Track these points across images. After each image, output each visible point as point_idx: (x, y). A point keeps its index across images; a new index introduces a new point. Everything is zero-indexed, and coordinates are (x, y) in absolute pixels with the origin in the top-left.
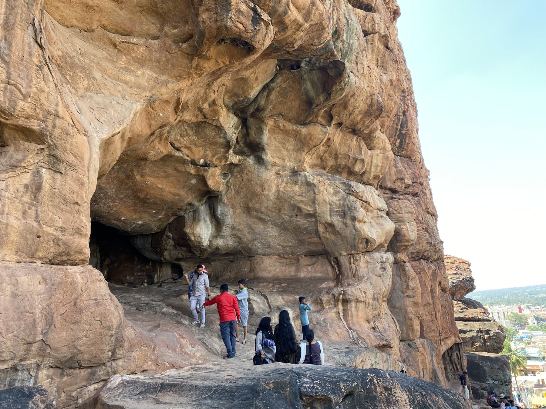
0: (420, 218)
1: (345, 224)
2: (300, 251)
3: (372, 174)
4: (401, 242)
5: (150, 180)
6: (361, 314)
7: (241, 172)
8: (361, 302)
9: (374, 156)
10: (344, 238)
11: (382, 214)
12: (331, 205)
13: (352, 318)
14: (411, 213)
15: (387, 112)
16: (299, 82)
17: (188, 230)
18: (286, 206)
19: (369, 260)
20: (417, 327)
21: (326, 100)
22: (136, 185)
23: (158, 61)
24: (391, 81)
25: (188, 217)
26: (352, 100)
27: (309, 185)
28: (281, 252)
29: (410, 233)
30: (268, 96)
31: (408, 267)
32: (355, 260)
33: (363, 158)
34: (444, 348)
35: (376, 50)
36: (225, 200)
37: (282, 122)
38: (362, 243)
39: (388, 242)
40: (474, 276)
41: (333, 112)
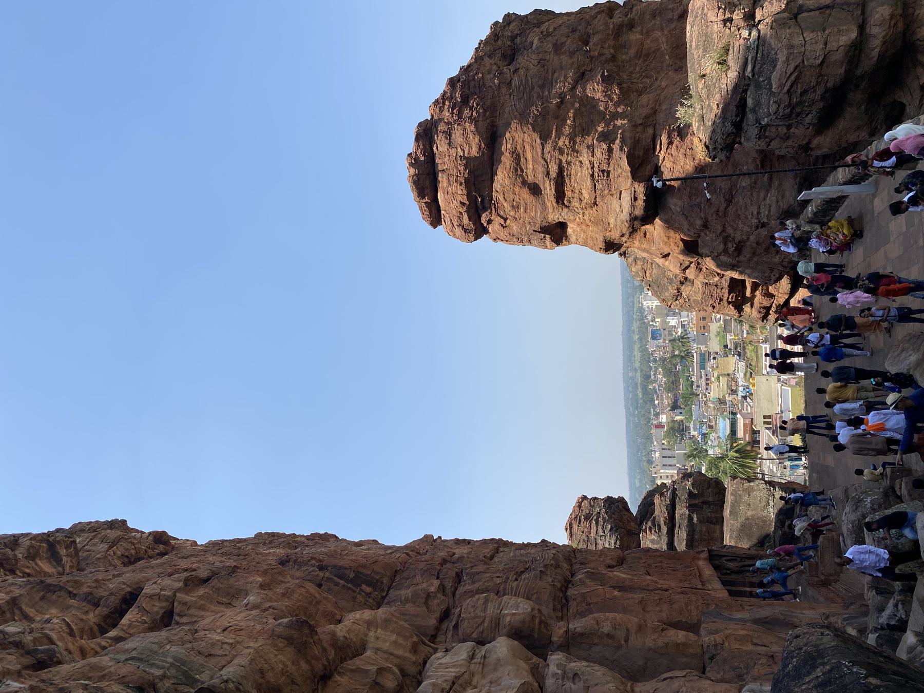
0: (498, 581)
3: (408, 655)
9: (377, 646)
14: (487, 600)
15: (311, 603)
20: (680, 636)
24: (262, 586)
29: (520, 611)
31: (577, 625)
33: (374, 668)
34: (718, 590)
39: (530, 654)
40: (602, 496)
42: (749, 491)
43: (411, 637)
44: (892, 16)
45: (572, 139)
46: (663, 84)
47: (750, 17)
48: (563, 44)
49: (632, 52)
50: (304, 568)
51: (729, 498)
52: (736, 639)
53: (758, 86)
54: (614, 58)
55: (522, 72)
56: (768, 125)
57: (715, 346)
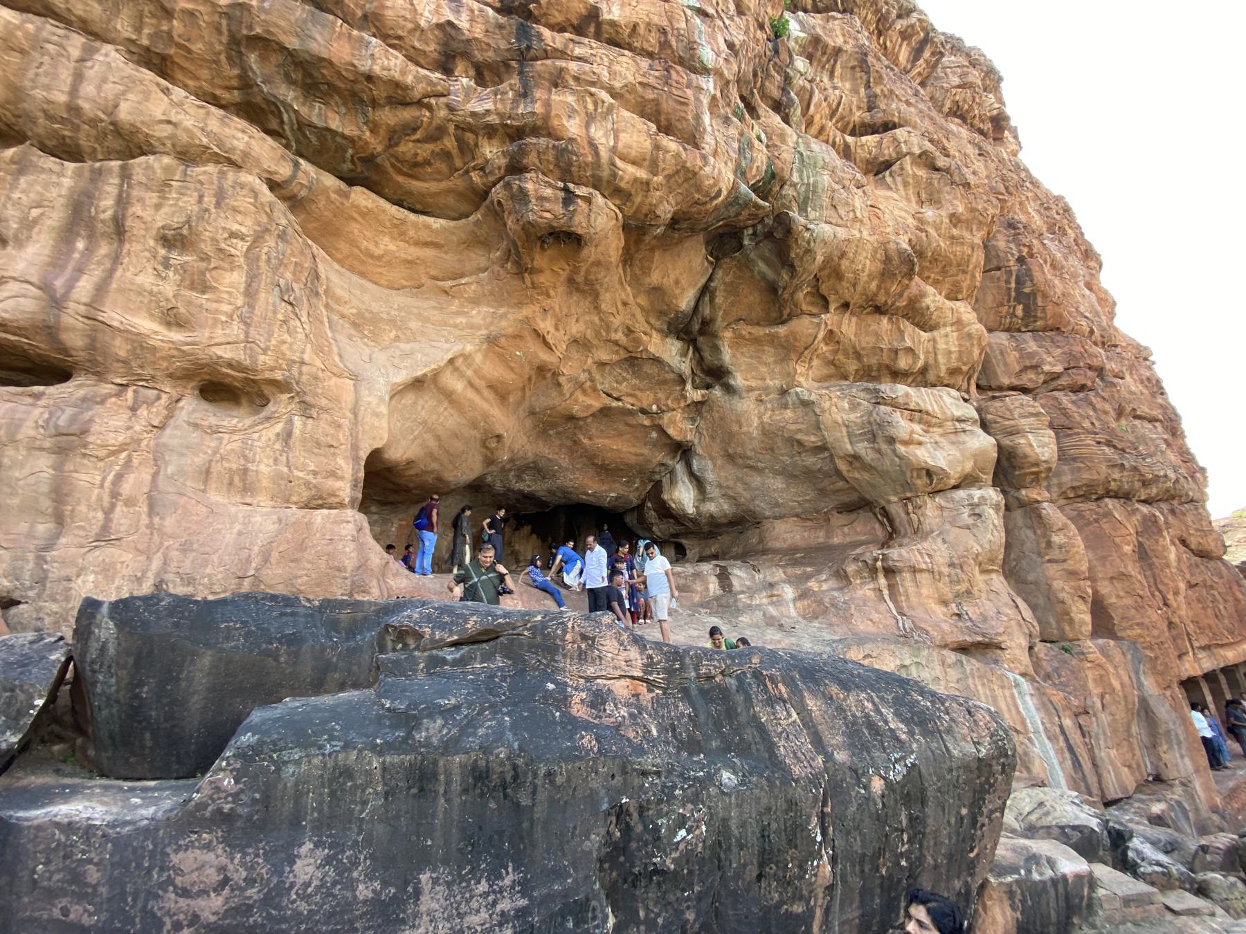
1: (879, 451)
2: (827, 505)
4: (1021, 468)
5: (601, 442)
6: (925, 591)
7: (711, 409)
8: (921, 571)
10: (883, 474)
11: (963, 425)
12: (847, 427)
13: (908, 597)
14: (1036, 415)
16: (747, 267)
17: (665, 497)
18: (779, 442)
19: (943, 504)
20: (1082, 615)
21: (792, 277)
22: (586, 451)
23: (491, 294)
25: (666, 481)
26: (845, 264)
27: (806, 404)
28: (799, 510)
29: (1038, 450)
30: (712, 300)
32: (915, 508)
33: (909, 343)
35: (911, 181)
36: (699, 450)
37: (745, 330)
38: (919, 477)
41: (824, 289)
43: (965, 364)
50: (1012, 245)
52: (1101, 676)
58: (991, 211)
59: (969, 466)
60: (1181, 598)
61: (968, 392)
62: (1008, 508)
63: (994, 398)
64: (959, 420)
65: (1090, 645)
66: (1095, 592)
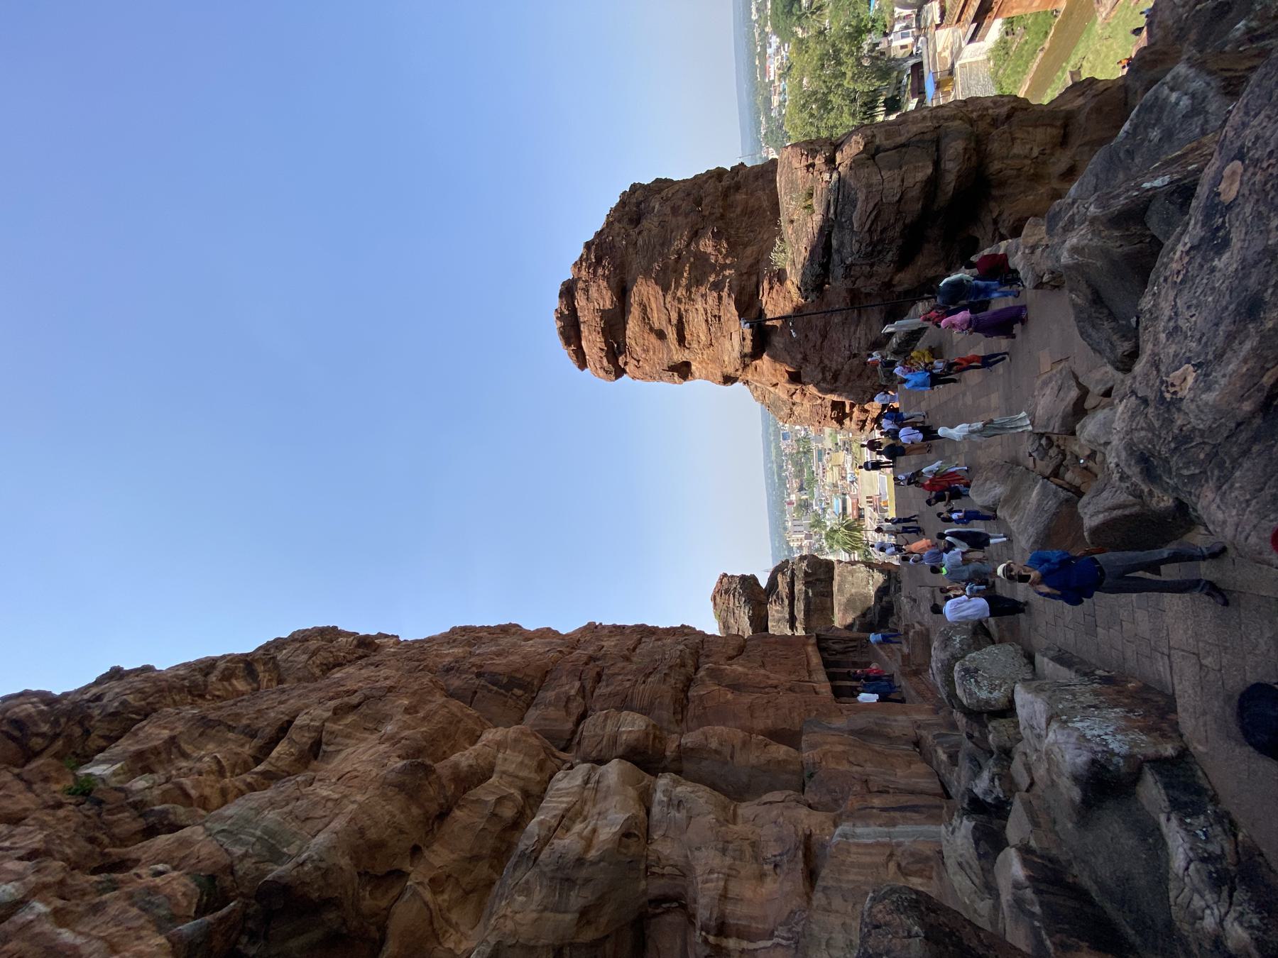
1: (587, 881)
3: (533, 775)
6: (749, 894)
8: (725, 888)
9: (504, 769)
11: (593, 780)
12: (545, 909)
14: (606, 717)
15: (451, 723)
20: (780, 751)
24: (407, 710)
29: (636, 728)
33: (492, 799)
38: (627, 847)
40: (738, 574)
41: (381, 869)
42: (852, 573)
43: (538, 755)
44: (965, 149)
45: (688, 289)
46: (765, 237)
47: (830, 161)
48: (679, 207)
49: (739, 210)
51: (836, 578)
53: (841, 227)
54: (722, 216)
55: (645, 233)
56: (852, 265)
57: (828, 444)
58: (426, 681)
59: (631, 792)
60: (772, 675)
61: (564, 762)
62: (679, 772)
63: (579, 743)
64: (586, 782)
65: (808, 755)
66: (762, 733)
